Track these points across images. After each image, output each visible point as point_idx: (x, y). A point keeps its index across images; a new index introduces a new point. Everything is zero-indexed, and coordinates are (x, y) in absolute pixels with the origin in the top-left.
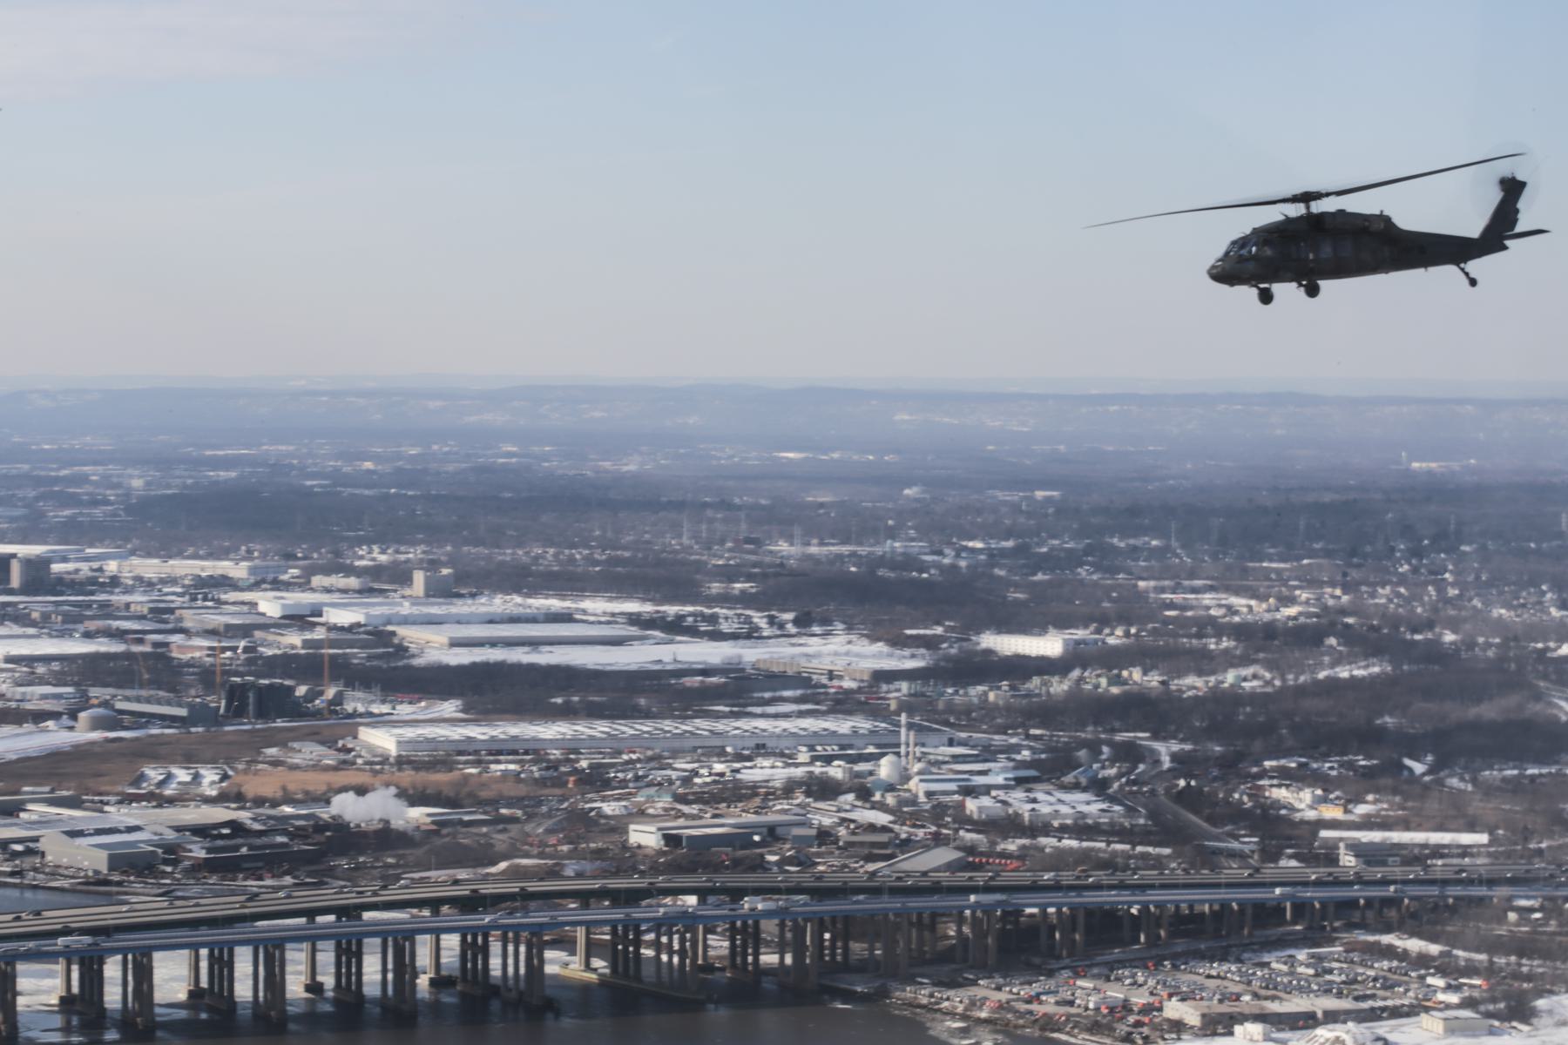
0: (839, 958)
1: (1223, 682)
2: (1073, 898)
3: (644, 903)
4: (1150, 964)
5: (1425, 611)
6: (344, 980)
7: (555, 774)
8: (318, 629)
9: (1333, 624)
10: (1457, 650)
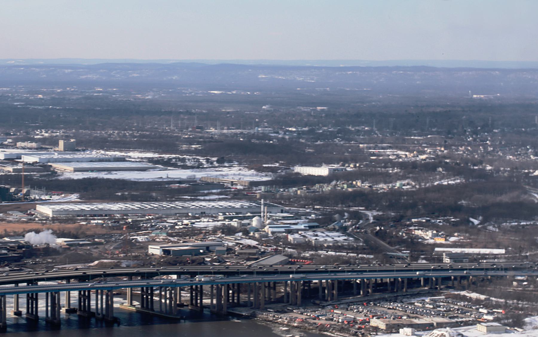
0: (236, 301)
1: (395, 186)
2: (333, 276)
3: (155, 278)
4: (365, 303)
5: (478, 157)
6: (30, 310)
7: (118, 225)
8: (20, 164)
9: (440, 162)
10: (492, 173)
